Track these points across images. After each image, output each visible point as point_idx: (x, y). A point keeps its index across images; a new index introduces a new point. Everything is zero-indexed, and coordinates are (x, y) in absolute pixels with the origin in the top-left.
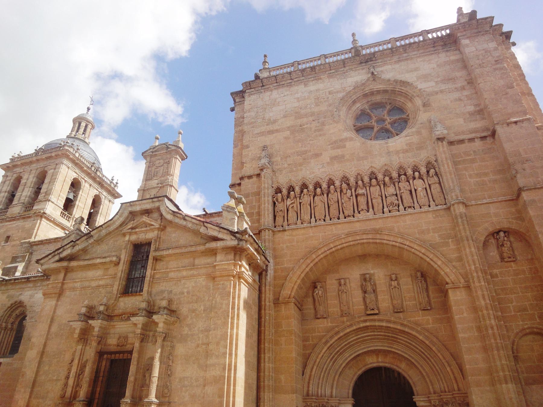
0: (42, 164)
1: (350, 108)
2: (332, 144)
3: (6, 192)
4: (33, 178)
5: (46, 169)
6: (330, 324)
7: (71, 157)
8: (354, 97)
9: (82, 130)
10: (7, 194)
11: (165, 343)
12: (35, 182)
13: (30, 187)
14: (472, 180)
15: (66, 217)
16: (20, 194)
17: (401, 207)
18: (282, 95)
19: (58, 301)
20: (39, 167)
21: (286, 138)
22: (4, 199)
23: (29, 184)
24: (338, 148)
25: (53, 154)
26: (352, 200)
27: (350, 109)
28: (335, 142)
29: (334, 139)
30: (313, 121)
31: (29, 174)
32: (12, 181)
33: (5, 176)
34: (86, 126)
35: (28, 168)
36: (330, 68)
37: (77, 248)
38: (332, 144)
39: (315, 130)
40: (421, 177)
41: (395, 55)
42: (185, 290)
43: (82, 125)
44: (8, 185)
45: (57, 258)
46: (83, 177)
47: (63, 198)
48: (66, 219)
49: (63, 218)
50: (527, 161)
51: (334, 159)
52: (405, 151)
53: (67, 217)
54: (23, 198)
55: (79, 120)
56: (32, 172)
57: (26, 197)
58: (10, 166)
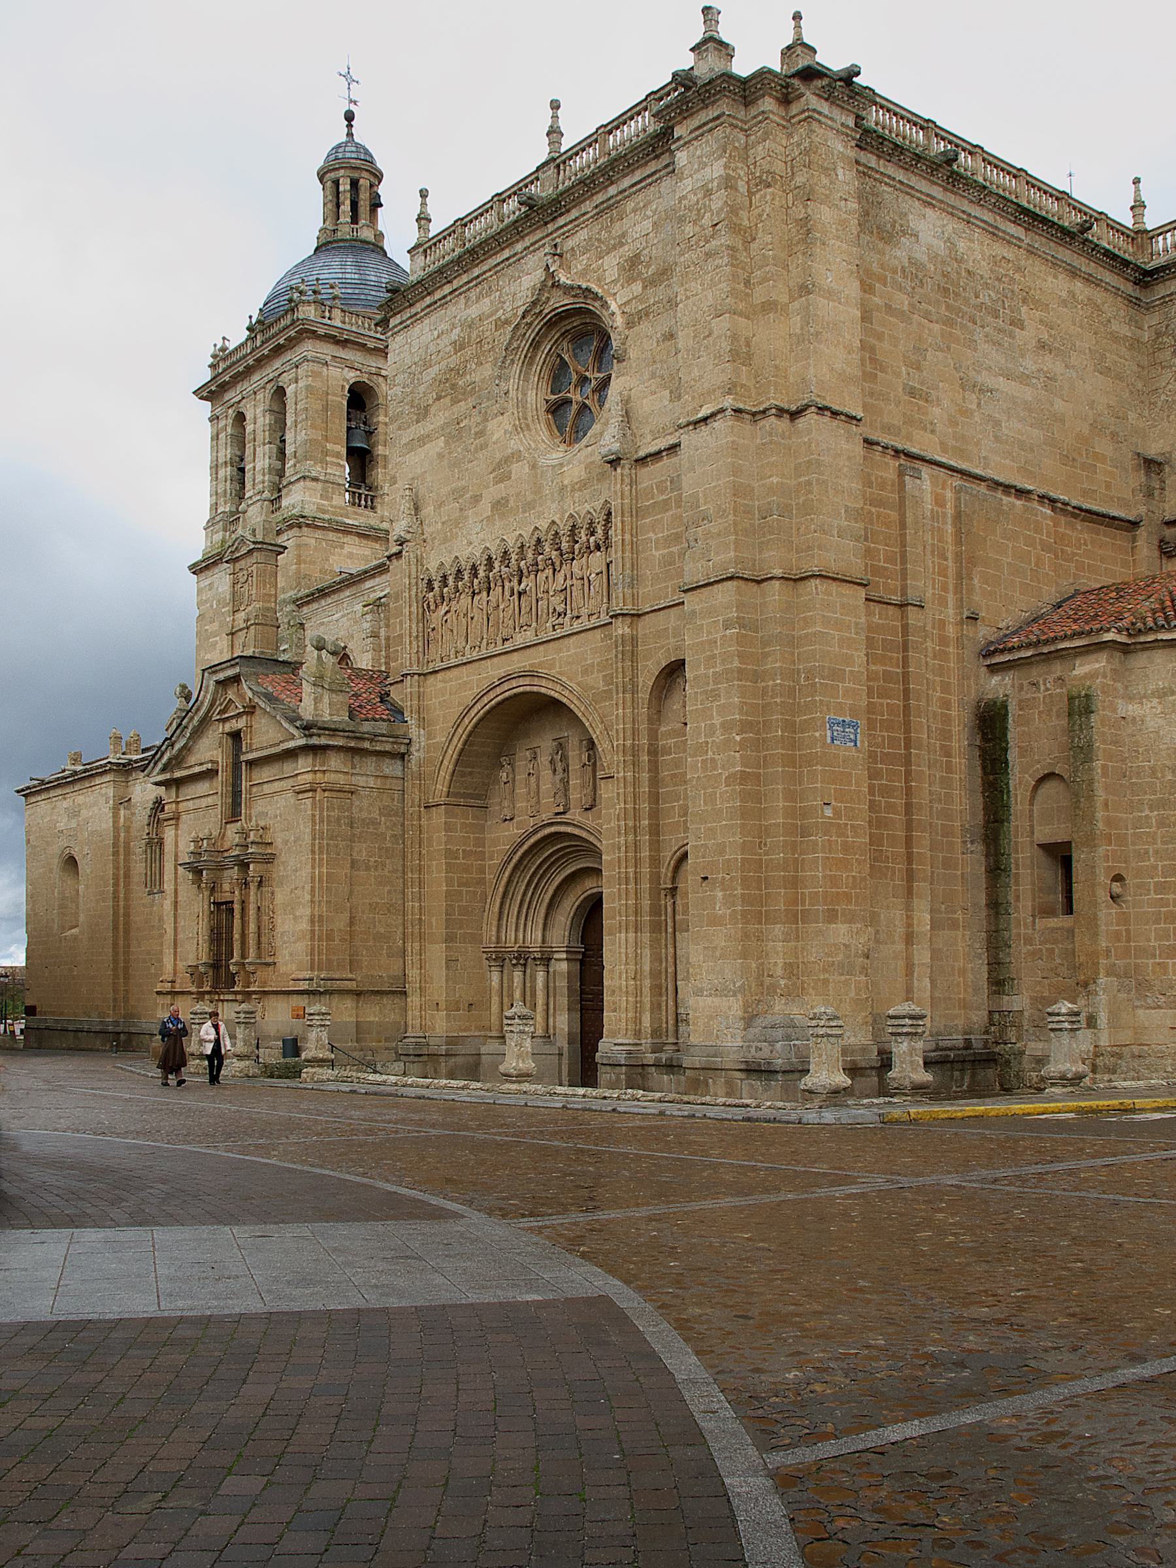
0: (269, 371)
1: (529, 361)
2: (494, 470)
3: (226, 462)
4: (264, 416)
5: (281, 384)
6: (516, 831)
7: (321, 332)
8: (531, 335)
9: (346, 207)
10: (229, 468)
11: (264, 889)
12: (270, 425)
13: (264, 444)
14: (657, 554)
15: (363, 502)
16: (252, 465)
17: (568, 616)
18: (436, 333)
19: (177, 829)
20: (266, 380)
21: (440, 456)
22: (229, 482)
23: (260, 438)
24: (500, 480)
25: (282, 341)
26: (512, 606)
27: (531, 364)
28: (499, 465)
29: (498, 456)
30: (474, 407)
31: (255, 406)
32: (229, 430)
33: (214, 419)
34: (354, 184)
35: (246, 386)
36: (499, 245)
37: (177, 746)
38: (494, 470)
39: (476, 434)
40: (598, 548)
41: (597, 193)
42: (278, 812)
43: (341, 188)
44: (226, 444)
45: (160, 766)
46: (374, 370)
47: (337, 455)
48: (366, 507)
49: (356, 509)
50: (703, 520)
51: (499, 505)
52: (583, 485)
53: (366, 502)
54: (259, 478)
55: (332, 175)
56: (258, 397)
57: (264, 475)
58: (213, 388)
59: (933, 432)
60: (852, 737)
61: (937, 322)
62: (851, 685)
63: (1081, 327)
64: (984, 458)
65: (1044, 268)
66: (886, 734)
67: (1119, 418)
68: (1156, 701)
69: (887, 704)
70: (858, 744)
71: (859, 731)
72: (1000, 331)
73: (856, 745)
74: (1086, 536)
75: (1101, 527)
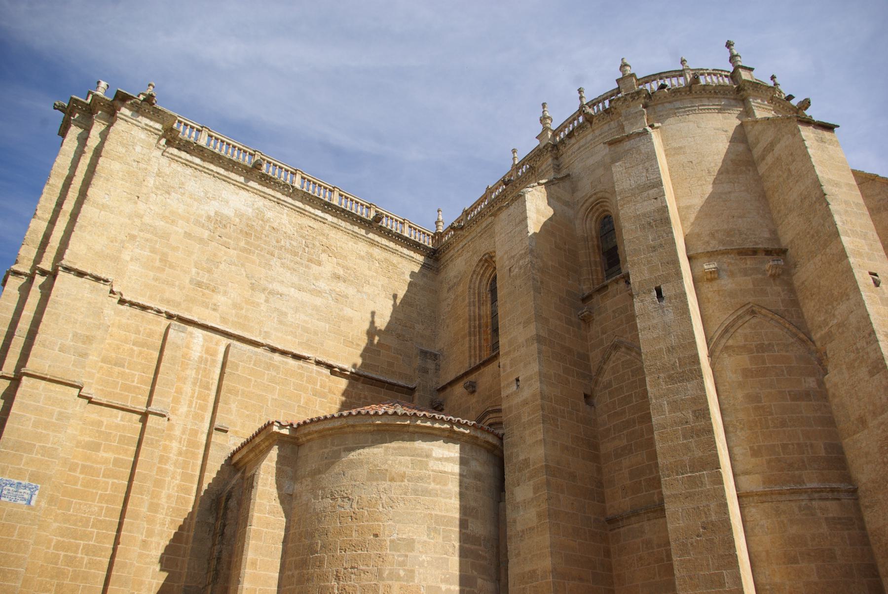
59: (214, 310)
60: (26, 496)
61: (235, 249)
62: (39, 456)
63: (377, 272)
64: (265, 332)
65: (346, 237)
66: (105, 505)
67: (406, 327)
68: (309, 479)
69: (113, 484)
70: (33, 503)
71: (37, 492)
72: (297, 263)
73: (29, 502)
74: (366, 393)
75: (382, 390)
